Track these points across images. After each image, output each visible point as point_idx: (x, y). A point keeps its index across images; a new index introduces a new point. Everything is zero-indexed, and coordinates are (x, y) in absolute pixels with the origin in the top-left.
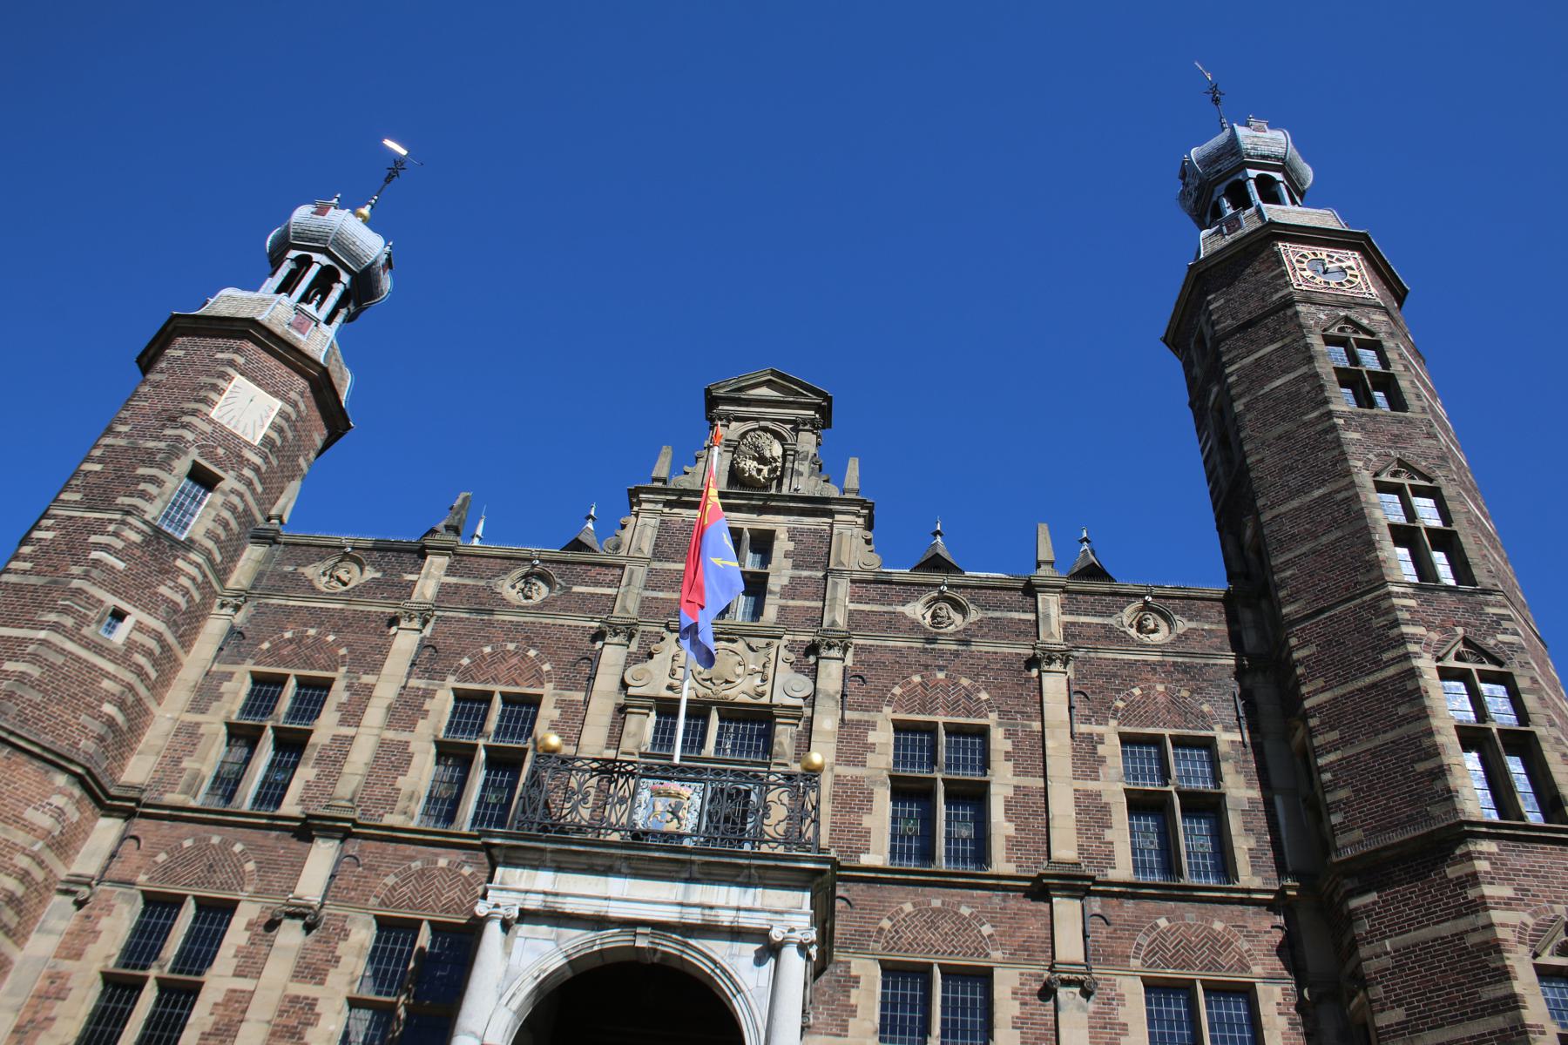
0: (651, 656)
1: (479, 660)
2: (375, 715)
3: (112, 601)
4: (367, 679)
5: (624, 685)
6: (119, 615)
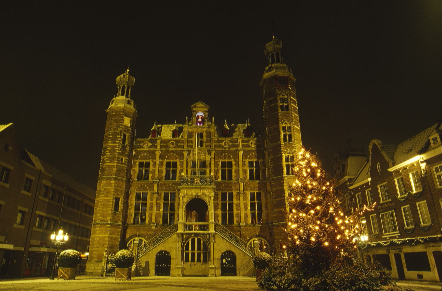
0: (190, 154)
1: (168, 156)
2: (157, 166)
3: (121, 157)
4: (154, 161)
5: (187, 159)
6: (122, 159)
